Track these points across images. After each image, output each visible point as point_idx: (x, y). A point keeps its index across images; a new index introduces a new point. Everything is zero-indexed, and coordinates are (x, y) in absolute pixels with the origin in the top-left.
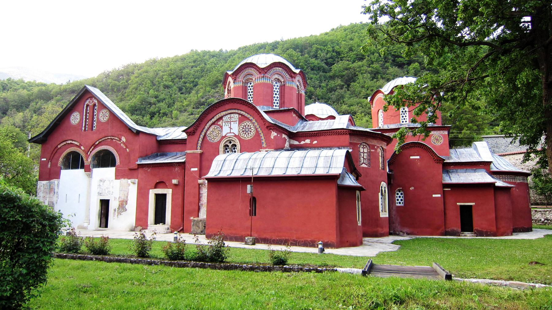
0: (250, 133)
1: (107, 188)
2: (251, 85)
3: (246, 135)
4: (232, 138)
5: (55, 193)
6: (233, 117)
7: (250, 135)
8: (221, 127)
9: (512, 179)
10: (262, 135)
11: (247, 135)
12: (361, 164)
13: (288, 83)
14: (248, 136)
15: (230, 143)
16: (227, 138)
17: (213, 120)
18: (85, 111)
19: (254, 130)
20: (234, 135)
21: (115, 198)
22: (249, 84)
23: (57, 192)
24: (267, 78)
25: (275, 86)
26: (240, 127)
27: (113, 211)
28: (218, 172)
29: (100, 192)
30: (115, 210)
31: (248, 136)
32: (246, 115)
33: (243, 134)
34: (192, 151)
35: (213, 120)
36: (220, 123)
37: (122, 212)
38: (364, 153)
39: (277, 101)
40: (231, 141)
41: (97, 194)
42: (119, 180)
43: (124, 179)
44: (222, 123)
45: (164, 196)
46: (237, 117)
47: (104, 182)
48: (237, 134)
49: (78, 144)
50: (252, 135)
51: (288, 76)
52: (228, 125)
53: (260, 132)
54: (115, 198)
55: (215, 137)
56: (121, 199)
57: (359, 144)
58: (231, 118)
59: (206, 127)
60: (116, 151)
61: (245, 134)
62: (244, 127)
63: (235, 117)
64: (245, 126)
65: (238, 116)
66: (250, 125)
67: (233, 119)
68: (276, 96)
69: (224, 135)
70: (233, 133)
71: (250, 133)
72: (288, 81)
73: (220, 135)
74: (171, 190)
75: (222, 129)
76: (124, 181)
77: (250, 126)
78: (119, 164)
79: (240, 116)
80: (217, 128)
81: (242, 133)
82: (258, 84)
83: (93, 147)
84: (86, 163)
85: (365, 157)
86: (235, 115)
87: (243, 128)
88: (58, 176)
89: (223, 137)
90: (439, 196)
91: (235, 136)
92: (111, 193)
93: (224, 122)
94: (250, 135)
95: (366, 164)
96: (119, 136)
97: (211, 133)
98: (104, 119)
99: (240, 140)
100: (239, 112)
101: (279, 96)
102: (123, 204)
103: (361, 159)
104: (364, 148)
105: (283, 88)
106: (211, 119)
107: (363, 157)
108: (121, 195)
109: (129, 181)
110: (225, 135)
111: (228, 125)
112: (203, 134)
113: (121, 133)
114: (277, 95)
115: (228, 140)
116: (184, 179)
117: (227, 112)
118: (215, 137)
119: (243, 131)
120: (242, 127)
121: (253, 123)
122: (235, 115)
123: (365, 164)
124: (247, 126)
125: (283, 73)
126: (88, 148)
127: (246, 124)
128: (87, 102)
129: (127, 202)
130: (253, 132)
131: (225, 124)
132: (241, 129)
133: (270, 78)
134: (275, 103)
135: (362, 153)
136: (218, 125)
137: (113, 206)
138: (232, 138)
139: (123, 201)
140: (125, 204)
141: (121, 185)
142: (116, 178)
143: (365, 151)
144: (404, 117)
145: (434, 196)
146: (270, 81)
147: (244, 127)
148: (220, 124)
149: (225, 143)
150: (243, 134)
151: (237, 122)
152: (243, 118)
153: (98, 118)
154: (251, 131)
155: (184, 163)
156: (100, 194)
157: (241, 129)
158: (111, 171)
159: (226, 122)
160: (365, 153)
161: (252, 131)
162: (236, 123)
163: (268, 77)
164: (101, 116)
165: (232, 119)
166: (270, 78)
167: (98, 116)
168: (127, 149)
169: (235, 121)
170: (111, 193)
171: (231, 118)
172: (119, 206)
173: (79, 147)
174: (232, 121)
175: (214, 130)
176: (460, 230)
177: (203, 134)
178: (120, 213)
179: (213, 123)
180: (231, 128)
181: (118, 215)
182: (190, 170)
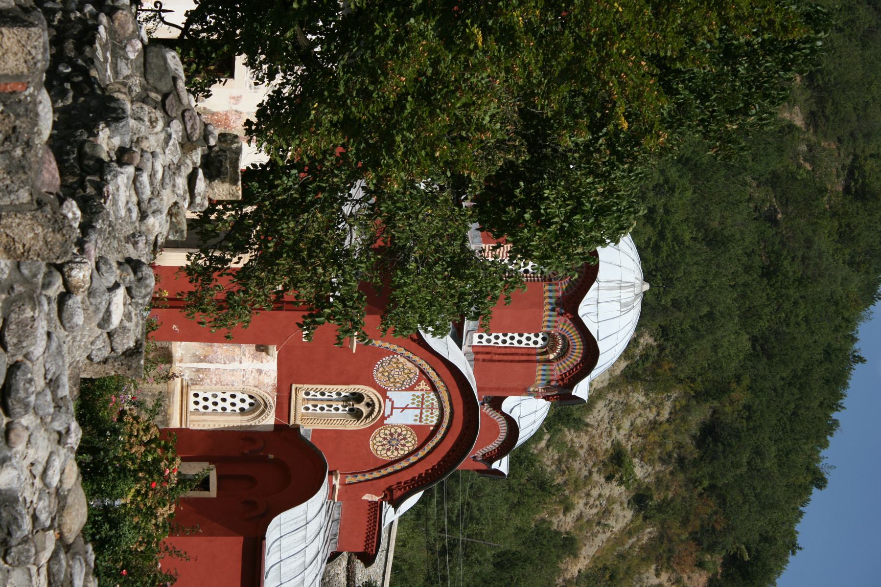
3: (381, 439)
4: (379, 411)
7: (380, 448)
8: (411, 388)
15: (368, 405)
17: (433, 375)
20: (386, 415)
21: (237, 99)
32: (431, 444)
33: (386, 434)
35: (433, 375)
36: (423, 385)
44: (422, 390)
48: (386, 422)
50: (379, 453)
52: (413, 403)
54: (237, 99)
55: (386, 374)
59: (417, 359)
62: (401, 437)
64: (405, 439)
66: (406, 448)
67: (428, 413)
69: (388, 394)
70: (391, 414)
73: (392, 385)
75: (406, 389)
79: (432, 428)
80: (410, 379)
81: (387, 432)
87: (400, 434)
89: (383, 392)
91: (384, 418)
93: (423, 395)
94: (380, 448)
97: (401, 366)
99: (372, 429)
100: (442, 431)
106: (434, 370)
110: (388, 397)
111: (413, 403)
112: (403, 350)
115: (372, 400)
117: (447, 405)
118: (386, 374)
119: (391, 434)
124: (403, 442)
127: (410, 440)
131: (418, 397)
132: (399, 431)
136: (419, 381)
138: (379, 411)
147: (401, 437)
151: (418, 423)
152: (425, 435)
154: (388, 450)
159: (423, 399)
161: (389, 453)
162: (416, 420)
169: (421, 418)
172: (213, 114)
175: (406, 371)
179: (422, 371)
180: (403, 409)
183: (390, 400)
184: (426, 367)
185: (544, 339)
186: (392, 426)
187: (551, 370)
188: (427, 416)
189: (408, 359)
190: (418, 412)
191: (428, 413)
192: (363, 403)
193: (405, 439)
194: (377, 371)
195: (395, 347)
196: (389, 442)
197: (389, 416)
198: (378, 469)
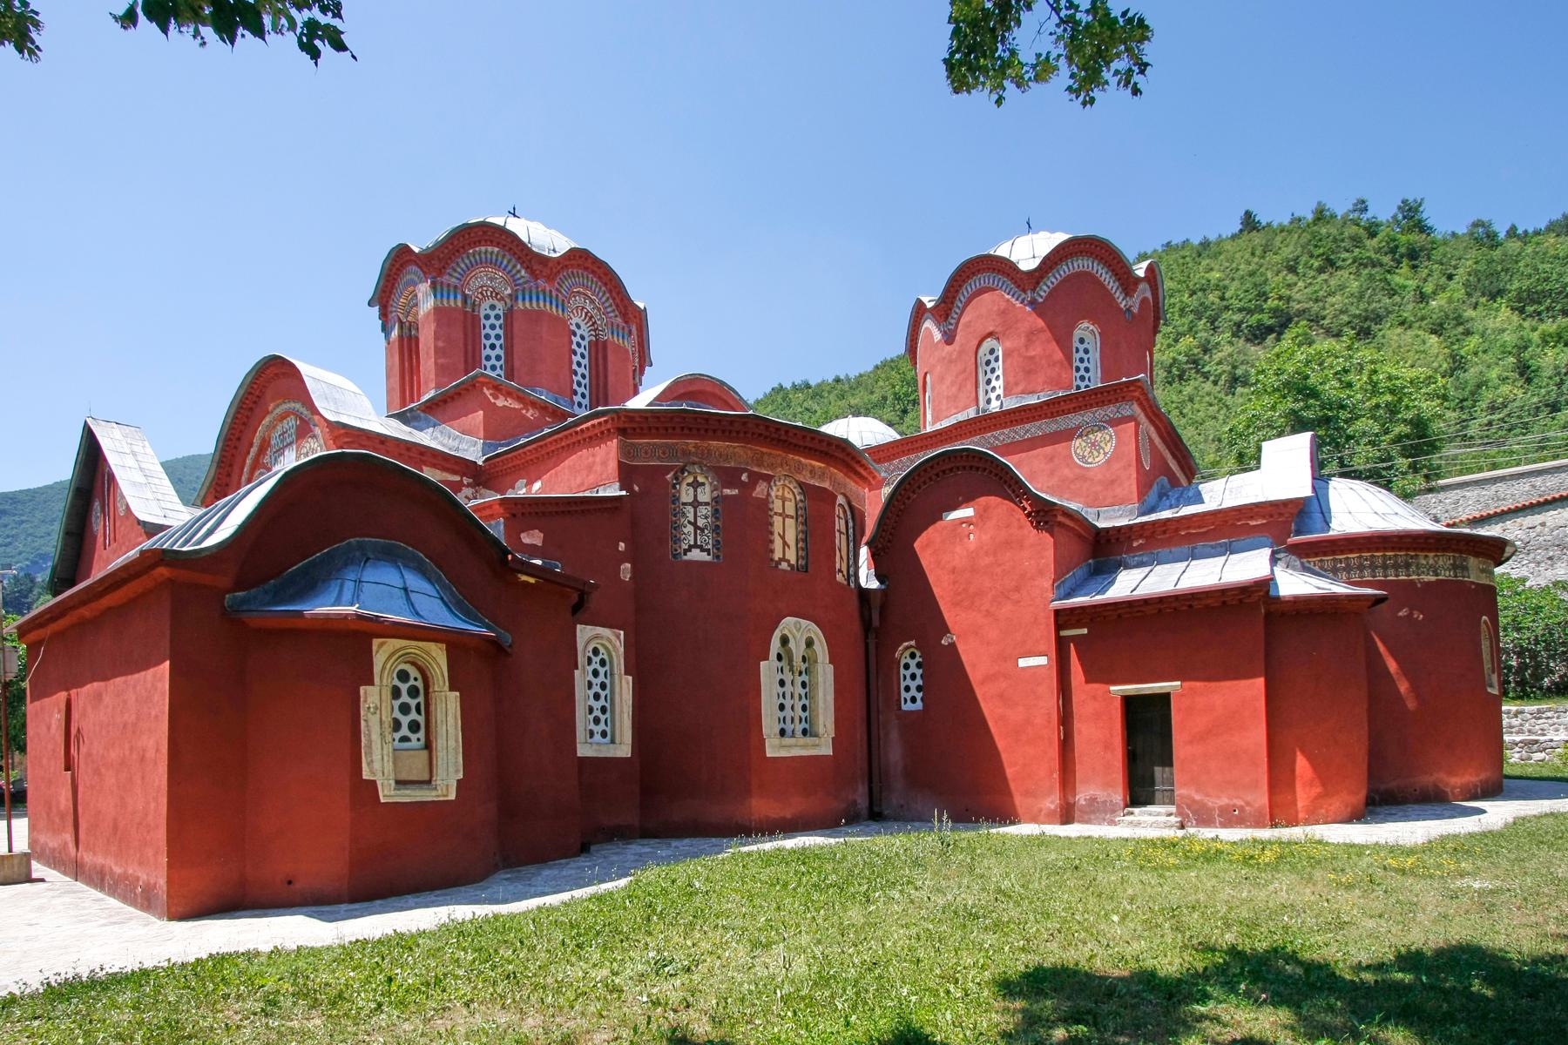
9: (1396, 567)
12: (689, 550)
13: (524, 299)
24: (445, 289)
38: (696, 504)
51: (523, 272)
57: (668, 469)
72: (523, 291)
85: (701, 522)
90: (1043, 661)
95: (708, 551)
103: (685, 530)
104: (696, 485)
107: (694, 524)
123: (703, 550)
125: (505, 262)
135: (690, 504)
143: (701, 498)
146: (459, 297)
160: (701, 504)
163: (449, 285)
166: (456, 287)
176: (1118, 797)
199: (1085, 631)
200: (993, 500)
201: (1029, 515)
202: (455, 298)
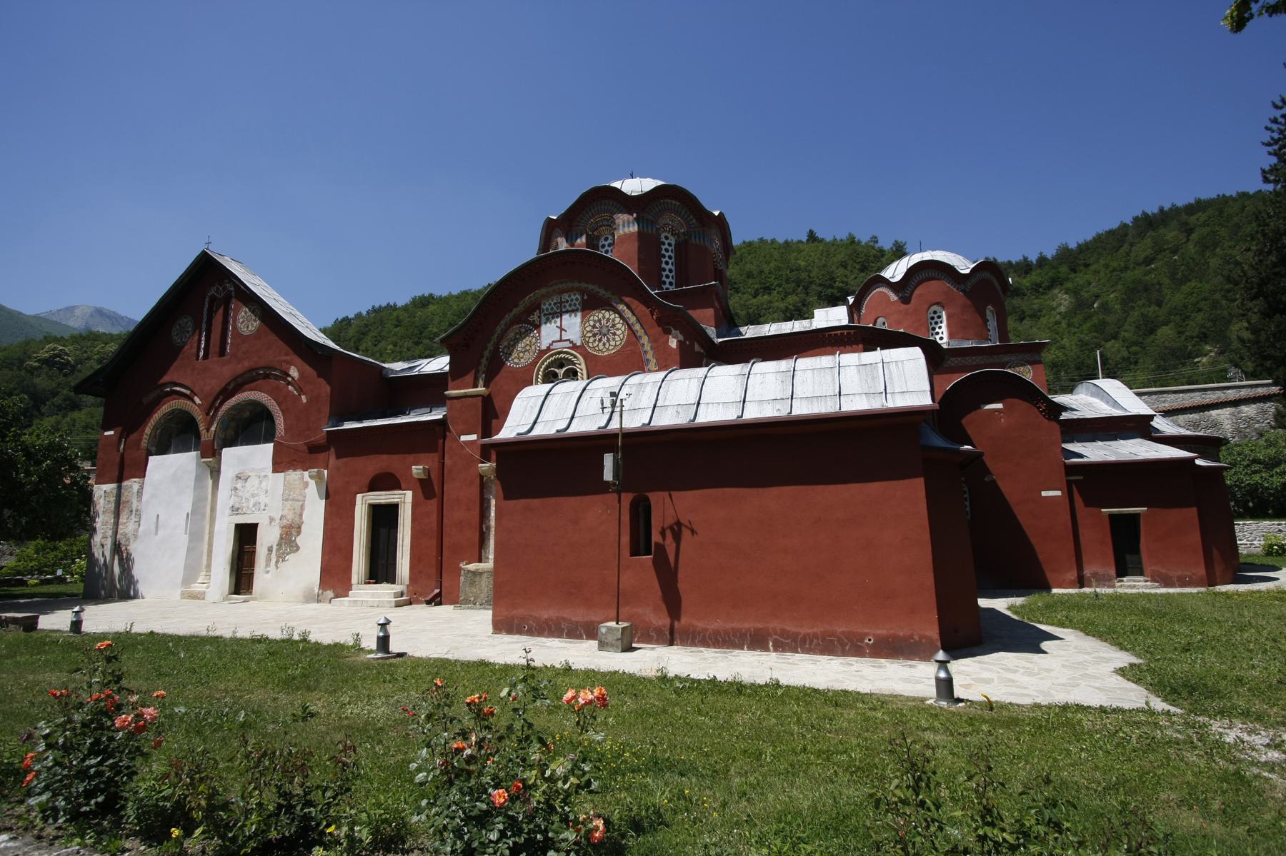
0: (614, 339)
1: (253, 495)
2: (606, 243)
3: (601, 344)
5: (132, 511)
6: (567, 301)
7: (612, 343)
10: (645, 340)
11: (604, 344)
14: (607, 345)
15: (561, 366)
16: (552, 355)
17: (515, 311)
18: (205, 312)
19: (623, 329)
20: (571, 345)
21: (272, 520)
22: (602, 239)
23: (137, 511)
25: (664, 244)
26: (587, 324)
27: (267, 552)
28: (529, 426)
29: (237, 506)
30: (270, 550)
31: (607, 345)
33: (595, 341)
34: (463, 391)
37: (288, 554)
39: (670, 279)
40: (564, 362)
41: (228, 511)
42: (283, 474)
43: (295, 470)
44: (539, 317)
45: (393, 509)
46: (577, 299)
47: (246, 480)
49: (188, 392)
50: (618, 343)
51: (694, 221)
53: (640, 332)
55: (521, 355)
56: (285, 522)
58: (561, 302)
59: (499, 330)
60: (275, 404)
61: (600, 340)
62: (597, 325)
63: (572, 300)
64: (599, 321)
65: (579, 297)
67: (567, 305)
68: (667, 268)
69: (544, 347)
70: (569, 340)
71: (614, 339)
73: (533, 347)
74: (409, 494)
76: (294, 475)
77: (614, 320)
78: (283, 433)
79: (586, 297)
81: (591, 340)
82: (625, 234)
83: (221, 397)
84: (206, 436)
86: (572, 297)
88: (140, 471)
89: (542, 353)
90: (1058, 493)
91: (575, 347)
92: (262, 507)
93: (545, 315)
94: (612, 343)
96: (284, 366)
98: (248, 327)
99: (587, 356)
101: (673, 268)
102: (291, 534)
105: (681, 248)
108: (286, 512)
109: (306, 474)
112: (490, 346)
113: (288, 358)
114: (670, 266)
116: (443, 463)
120: (592, 323)
121: (622, 317)
122: (572, 297)
126: (211, 400)
128: (212, 292)
129: (299, 528)
130: (621, 336)
133: (652, 222)
134: (664, 270)
136: (529, 323)
137: (267, 538)
139: (290, 527)
140: (294, 533)
141: (287, 485)
142: (275, 471)
144: (937, 330)
145: (1044, 494)
147: (597, 325)
148: (534, 321)
149: (548, 367)
150: (595, 341)
152: (590, 305)
153: (235, 327)
154: (614, 334)
155: (442, 423)
156: (235, 510)
157: (588, 329)
158: (265, 452)
159: (550, 314)
161: (618, 332)
164: (241, 320)
165: (565, 307)
166: (652, 222)
167: (235, 321)
168: (303, 397)
170: (262, 507)
171: (561, 302)
172: (281, 538)
173: (191, 399)
174: (564, 310)
175: (518, 337)
177: (490, 346)
178: (281, 558)
180: (562, 329)
181: (277, 562)
182: (457, 440)
183: (551, 345)
184: (508, 317)
185: (606, 239)
186: (584, 336)
187: (624, 222)
188: (570, 305)
189: (501, 337)
190: (566, 317)
191: (567, 305)
192: (556, 370)
193: (599, 321)
194: (518, 364)
195: (487, 353)
196: (604, 335)
197: (571, 342)
198: (638, 338)
199: (1082, 478)
200: (1016, 401)
201: (1041, 412)
202: (652, 229)
